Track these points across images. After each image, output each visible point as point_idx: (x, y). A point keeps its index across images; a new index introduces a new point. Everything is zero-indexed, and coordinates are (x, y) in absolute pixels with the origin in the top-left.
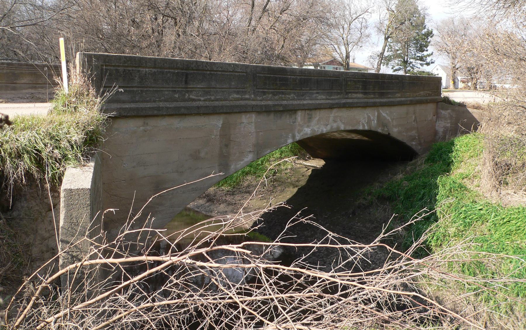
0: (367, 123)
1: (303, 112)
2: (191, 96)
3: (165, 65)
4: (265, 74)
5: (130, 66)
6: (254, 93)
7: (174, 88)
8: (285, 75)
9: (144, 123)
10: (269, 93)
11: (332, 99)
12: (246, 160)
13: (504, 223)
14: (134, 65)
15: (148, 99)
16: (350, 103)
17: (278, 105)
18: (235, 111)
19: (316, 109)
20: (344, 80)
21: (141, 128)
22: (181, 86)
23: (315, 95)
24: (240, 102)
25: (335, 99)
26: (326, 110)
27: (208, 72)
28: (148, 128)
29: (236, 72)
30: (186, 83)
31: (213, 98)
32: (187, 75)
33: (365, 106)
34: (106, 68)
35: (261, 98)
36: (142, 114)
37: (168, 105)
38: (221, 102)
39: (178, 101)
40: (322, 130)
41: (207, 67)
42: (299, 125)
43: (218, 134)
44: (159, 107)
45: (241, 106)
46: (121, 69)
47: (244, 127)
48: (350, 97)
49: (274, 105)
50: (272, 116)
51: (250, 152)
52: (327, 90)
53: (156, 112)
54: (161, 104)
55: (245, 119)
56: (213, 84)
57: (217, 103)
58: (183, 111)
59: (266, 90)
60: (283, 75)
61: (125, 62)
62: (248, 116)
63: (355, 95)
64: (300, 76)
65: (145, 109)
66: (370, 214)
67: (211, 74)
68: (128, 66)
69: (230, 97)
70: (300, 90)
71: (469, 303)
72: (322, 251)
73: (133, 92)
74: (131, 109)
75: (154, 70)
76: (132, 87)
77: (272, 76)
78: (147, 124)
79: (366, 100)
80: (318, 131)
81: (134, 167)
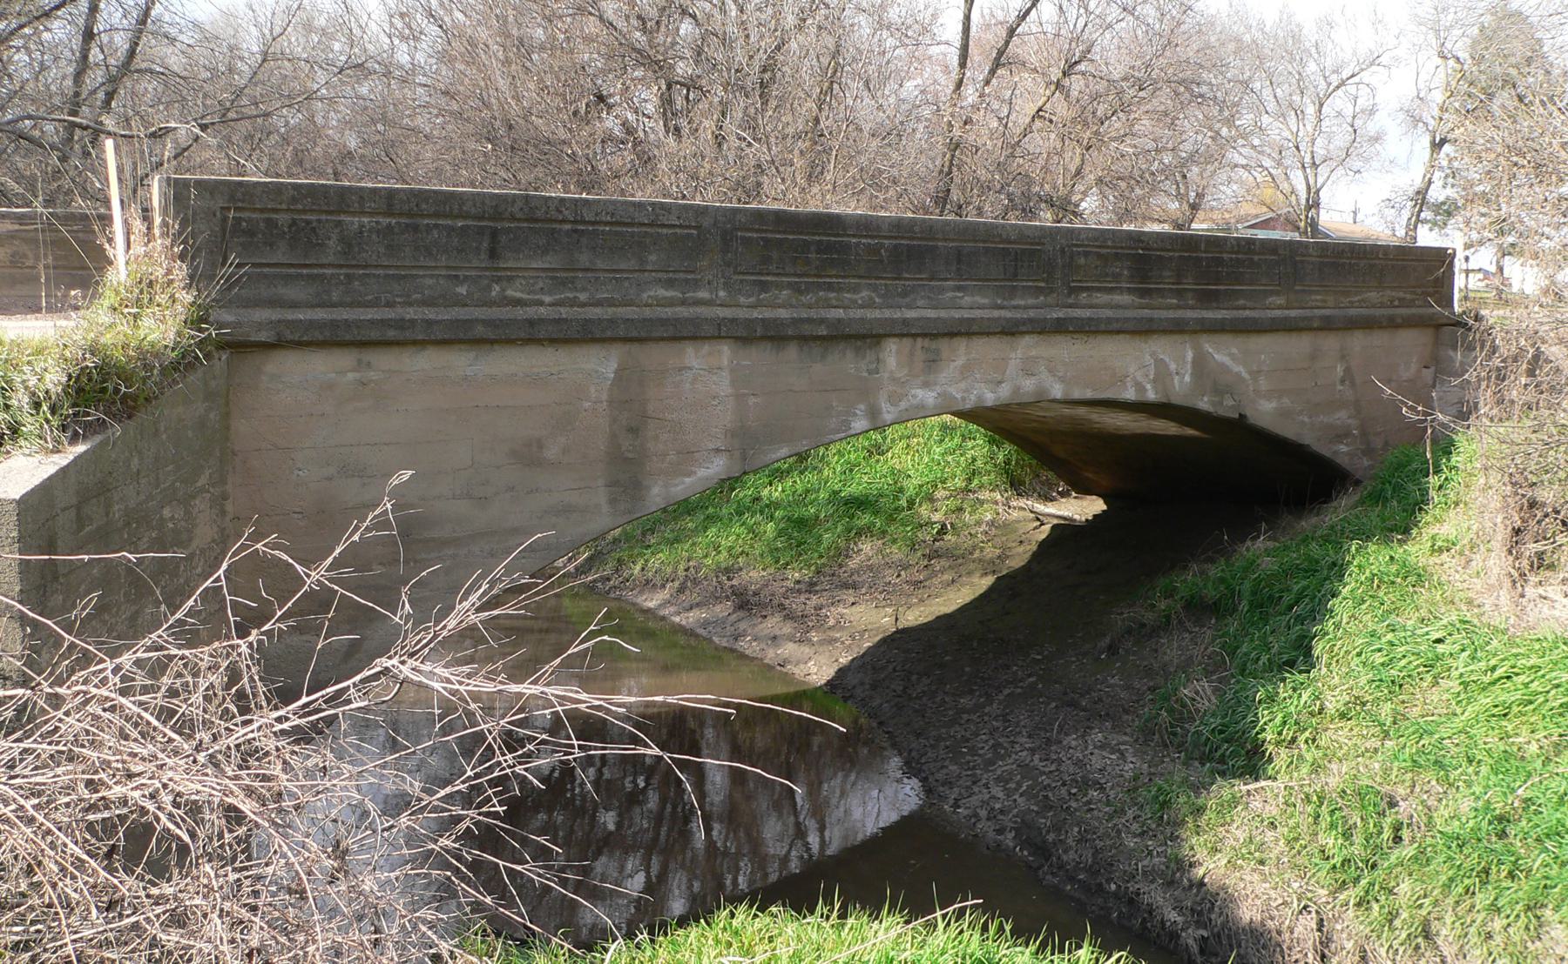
0: (1154, 381)
1: (907, 342)
2: (510, 293)
3: (424, 206)
4: (766, 231)
5: (312, 211)
6: (727, 286)
7: (455, 268)
8: (838, 235)
9: (359, 361)
10: (780, 286)
11: (1015, 307)
12: (702, 473)
13: (1493, 683)
14: (325, 208)
15: (370, 297)
16: (1082, 319)
17: (810, 321)
18: (655, 334)
19: (952, 335)
20: (1063, 251)
21: (351, 376)
22: (475, 263)
23: (950, 294)
24: (678, 309)
25: (1026, 308)
26: (994, 340)
27: (568, 227)
28: (372, 375)
29: (664, 226)
30: (493, 254)
31: (583, 297)
32: (494, 234)
33: (1145, 330)
34: (237, 215)
35: (751, 300)
36: (348, 337)
37: (430, 314)
38: (611, 310)
39: (466, 305)
40: (979, 398)
41: (561, 212)
42: (894, 379)
43: (604, 397)
44: (403, 320)
45: (676, 322)
46: (283, 219)
47: (695, 379)
48: (1084, 302)
49: (796, 322)
50: (792, 352)
51: (717, 450)
52: (995, 280)
53: (391, 334)
54: (411, 313)
55: (693, 357)
56: (584, 259)
57: (598, 310)
58: (480, 331)
59: (769, 278)
60: (829, 235)
61: (294, 200)
62: (706, 348)
63: (1102, 298)
64: (896, 238)
65: (359, 324)
66: (1156, 651)
67: (576, 231)
68: (304, 211)
69: (645, 296)
70: (896, 279)
71: (1305, 907)
72: (981, 752)
73: (322, 277)
74: (312, 324)
75: (385, 221)
76: (322, 266)
77: (791, 237)
78: (369, 364)
79: (1146, 313)
80: (963, 399)
81: (330, 479)
